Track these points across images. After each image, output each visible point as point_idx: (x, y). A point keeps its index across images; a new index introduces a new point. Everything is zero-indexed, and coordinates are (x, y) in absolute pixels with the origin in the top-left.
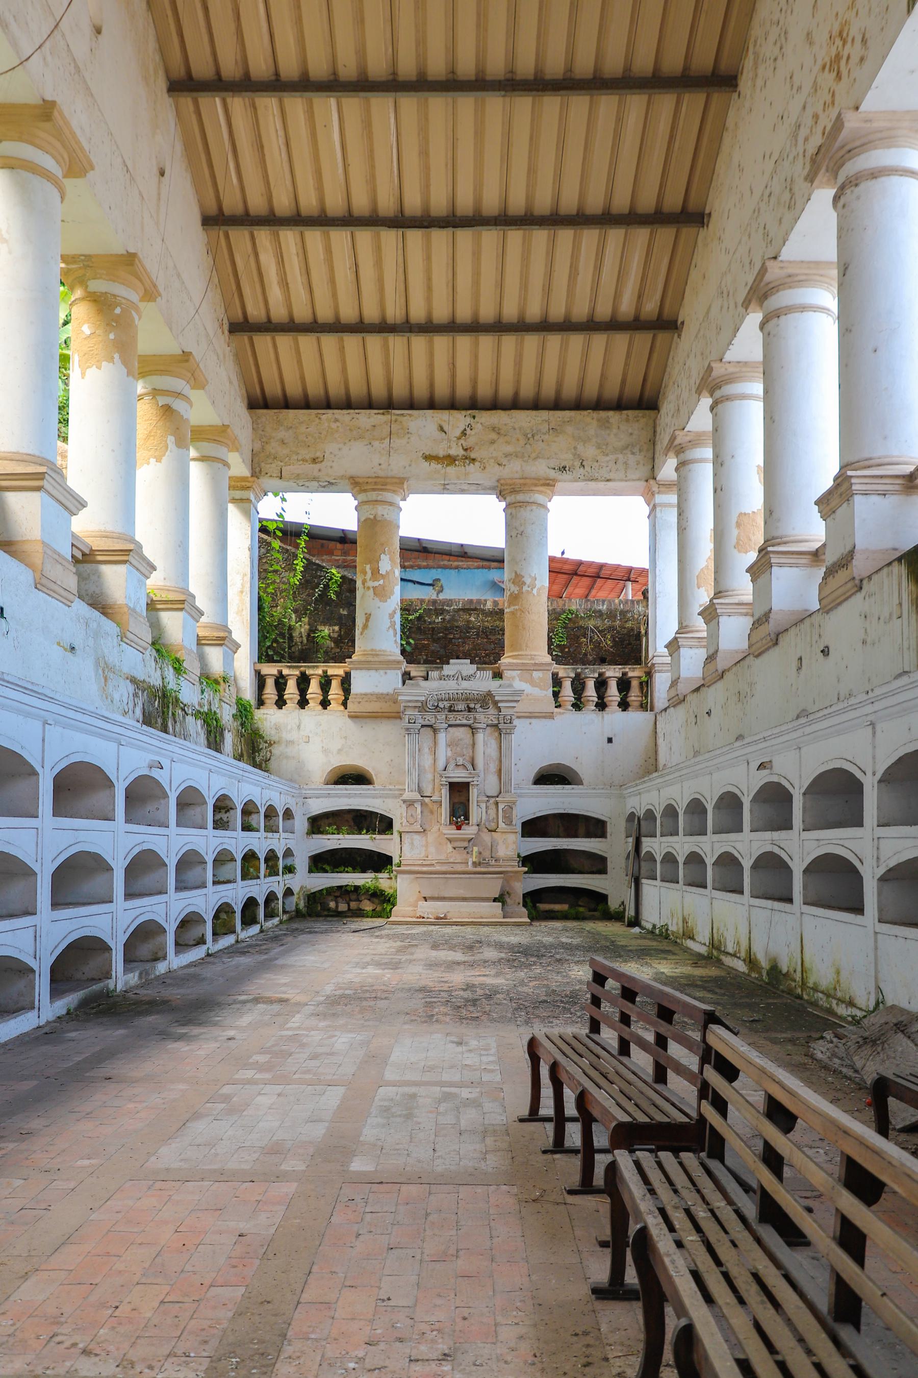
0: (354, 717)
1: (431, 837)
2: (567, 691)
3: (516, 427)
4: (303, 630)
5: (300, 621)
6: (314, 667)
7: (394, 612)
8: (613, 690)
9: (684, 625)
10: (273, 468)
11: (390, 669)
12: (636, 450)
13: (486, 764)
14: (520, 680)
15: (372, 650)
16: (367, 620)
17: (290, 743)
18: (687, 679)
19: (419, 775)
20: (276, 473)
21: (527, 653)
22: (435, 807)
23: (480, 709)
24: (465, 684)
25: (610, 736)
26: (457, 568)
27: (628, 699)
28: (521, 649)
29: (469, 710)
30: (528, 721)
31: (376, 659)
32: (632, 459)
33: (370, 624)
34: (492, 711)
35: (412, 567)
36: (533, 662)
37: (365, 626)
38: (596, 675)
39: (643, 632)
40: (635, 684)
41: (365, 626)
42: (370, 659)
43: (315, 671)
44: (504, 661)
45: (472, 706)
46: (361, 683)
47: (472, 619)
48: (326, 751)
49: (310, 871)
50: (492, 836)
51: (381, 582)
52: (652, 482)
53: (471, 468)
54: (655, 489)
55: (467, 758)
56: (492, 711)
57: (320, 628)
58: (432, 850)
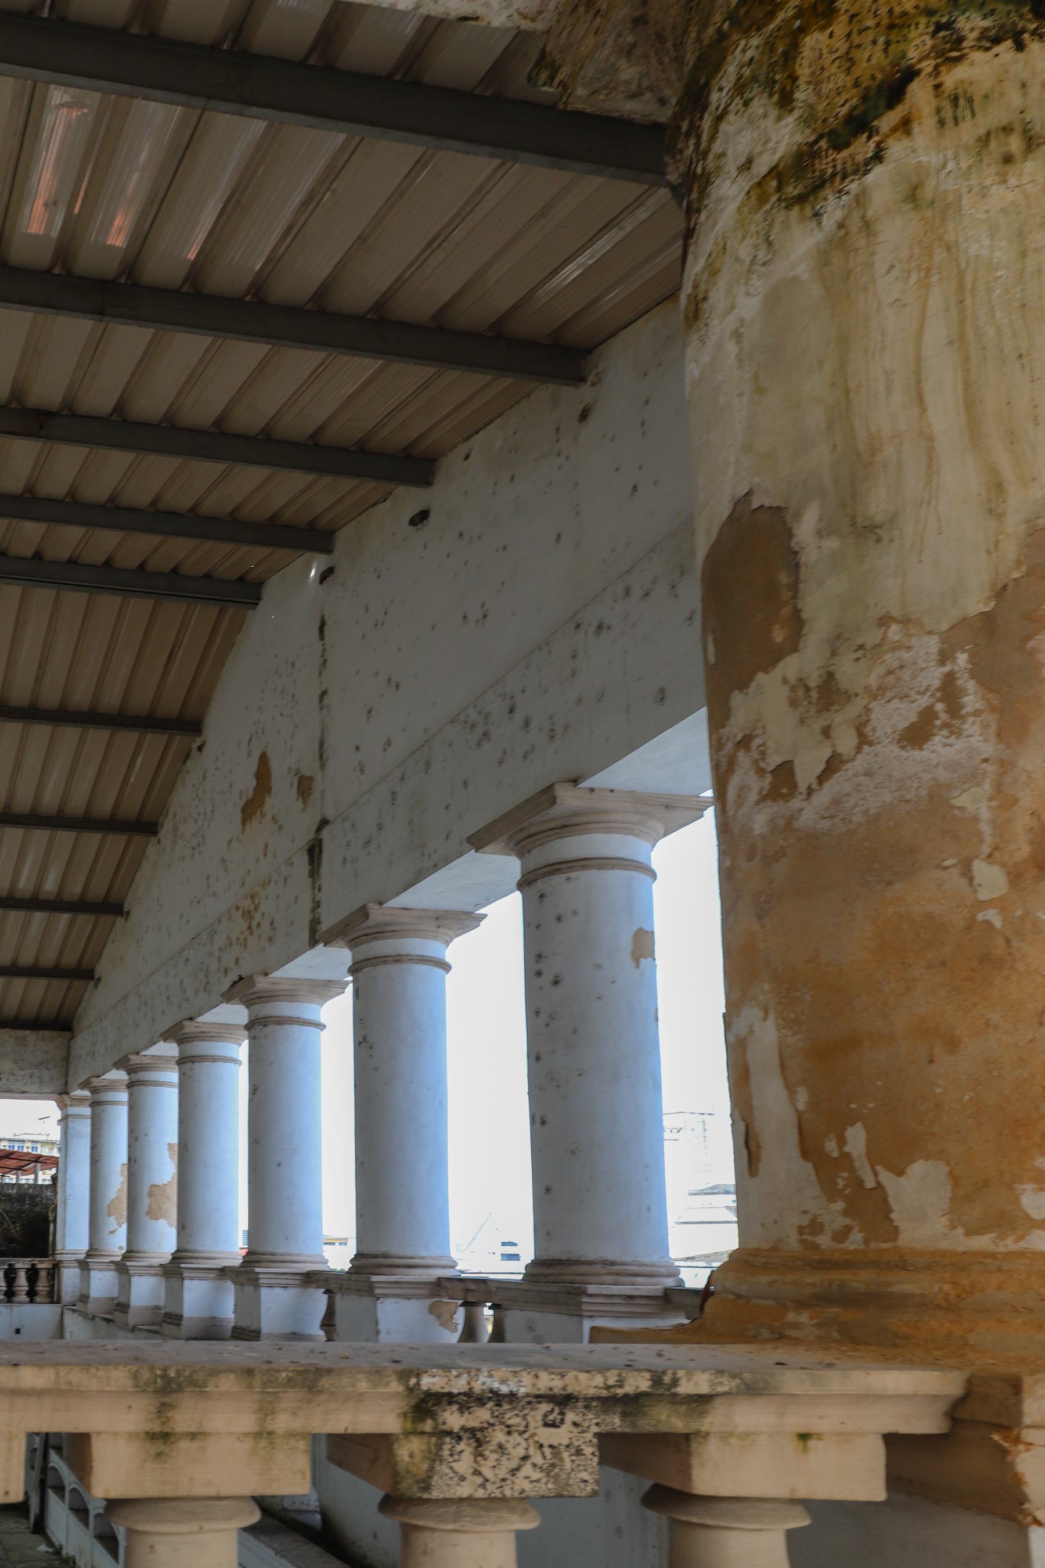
8: (22, 1280)
9: (95, 1247)
18: (96, 1299)
25: (18, 1327)
32: (47, 1075)
39: (51, 1218)
40: (43, 1274)
52: (65, 1096)
54: (68, 1102)
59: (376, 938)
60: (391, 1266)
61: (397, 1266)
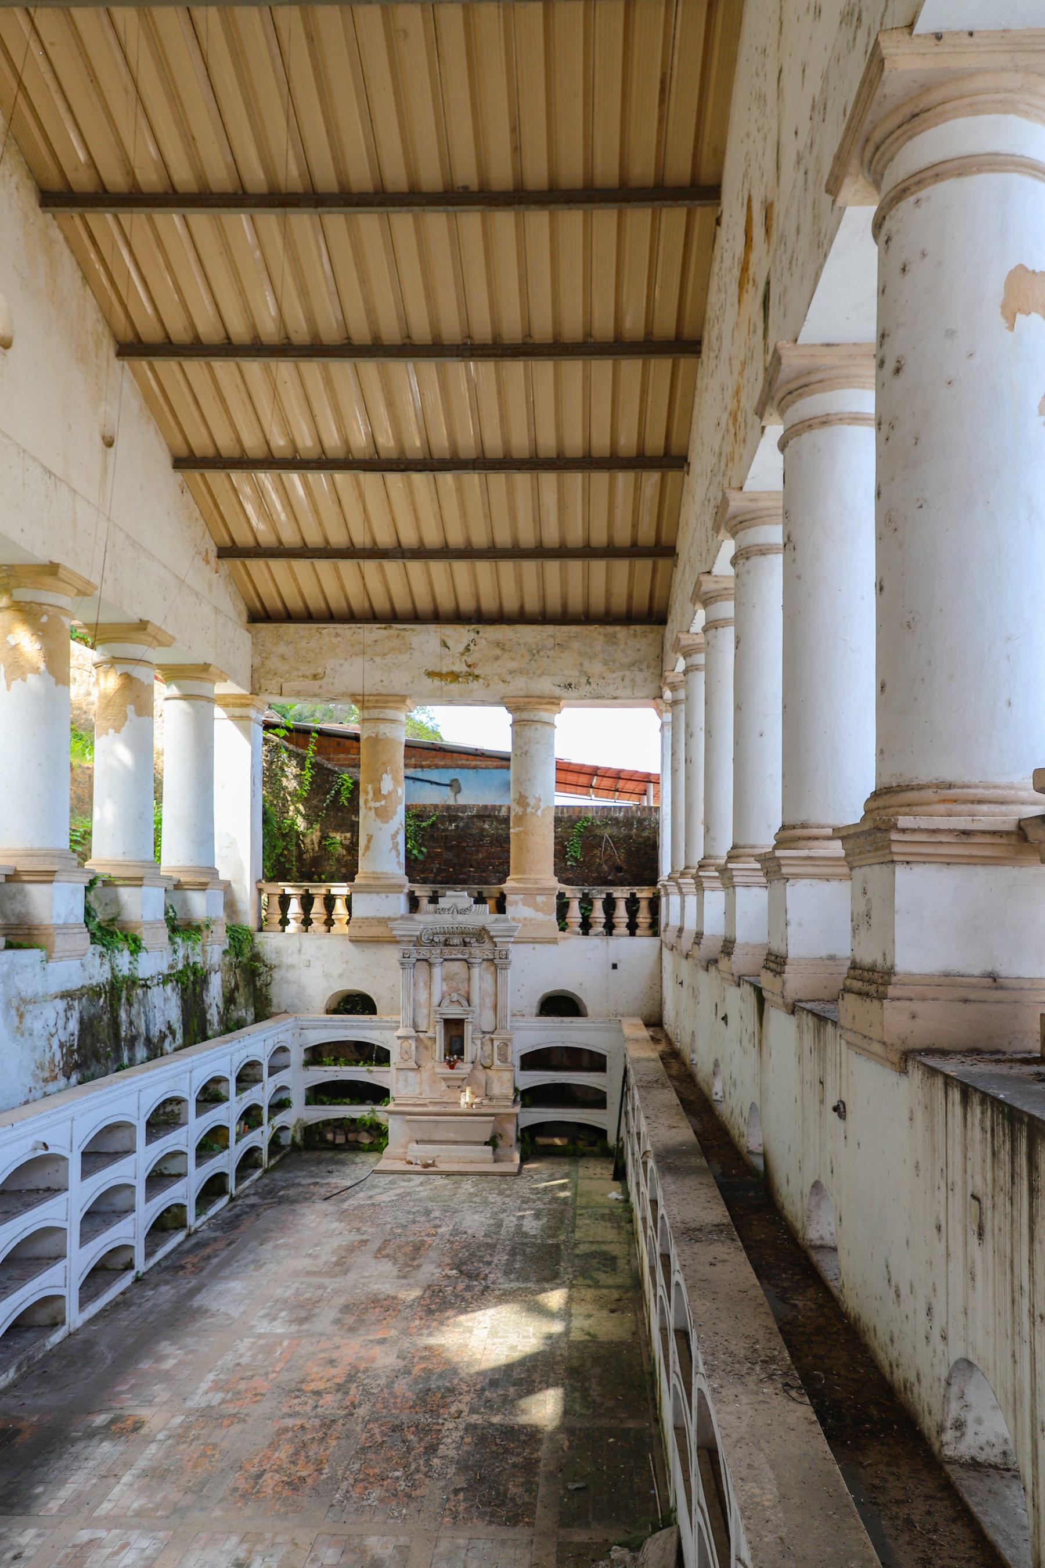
0: (355, 941)
1: (425, 1074)
2: (575, 913)
3: (521, 642)
4: (314, 837)
5: (311, 827)
6: (317, 887)
7: (397, 833)
8: (621, 913)
10: (273, 684)
11: (391, 892)
12: (644, 666)
13: (482, 999)
14: (524, 905)
15: (374, 873)
16: (369, 841)
17: (291, 967)
19: (414, 1010)
20: (277, 690)
21: (532, 876)
22: (429, 1043)
23: (476, 944)
24: (460, 918)
26: (475, 767)
27: (638, 920)
28: (524, 873)
29: (465, 944)
30: (532, 946)
31: (377, 882)
32: (639, 677)
33: (371, 845)
34: (487, 945)
35: (429, 767)
36: (536, 886)
37: (367, 848)
38: (604, 896)
40: (644, 904)
41: (367, 848)
42: (372, 882)
43: (319, 890)
44: (509, 884)
45: (467, 940)
46: (363, 906)
47: (487, 826)
48: (327, 976)
49: (307, 1103)
50: (487, 1075)
51: (383, 803)
53: (475, 685)
55: (463, 993)
56: (487, 945)
57: (332, 835)
58: (426, 1087)
59: (800, 395)
60: (809, 838)
61: (816, 838)
